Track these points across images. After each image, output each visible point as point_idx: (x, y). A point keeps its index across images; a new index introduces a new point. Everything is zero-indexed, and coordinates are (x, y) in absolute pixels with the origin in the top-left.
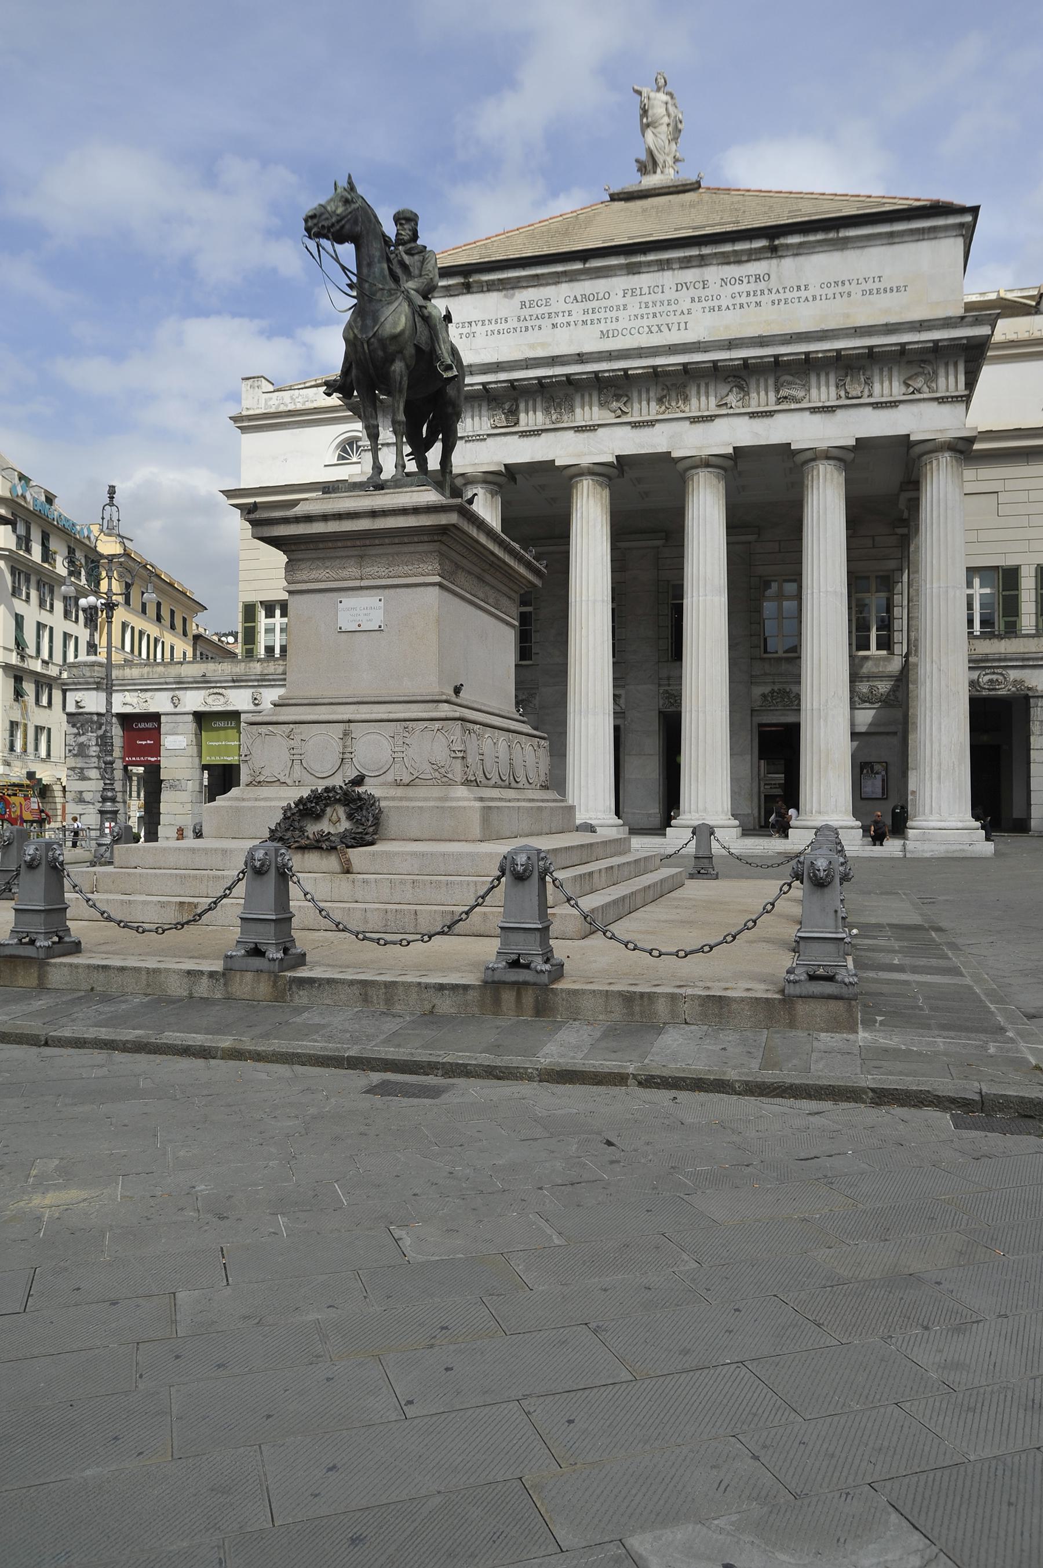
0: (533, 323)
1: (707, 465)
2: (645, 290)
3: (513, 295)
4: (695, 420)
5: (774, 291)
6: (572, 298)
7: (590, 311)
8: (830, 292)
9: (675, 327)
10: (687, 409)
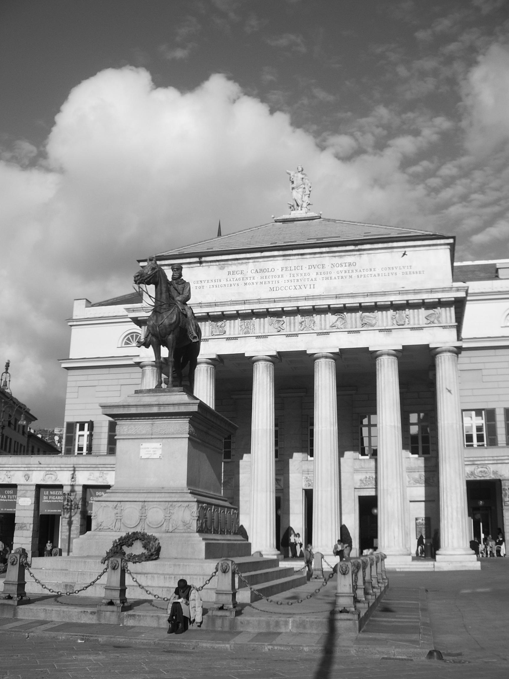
1: (326, 357)
2: (293, 268)
3: (224, 268)
4: (319, 334)
5: (358, 271)
6: (255, 271)
7: (264, 277)
8: (386, 272)
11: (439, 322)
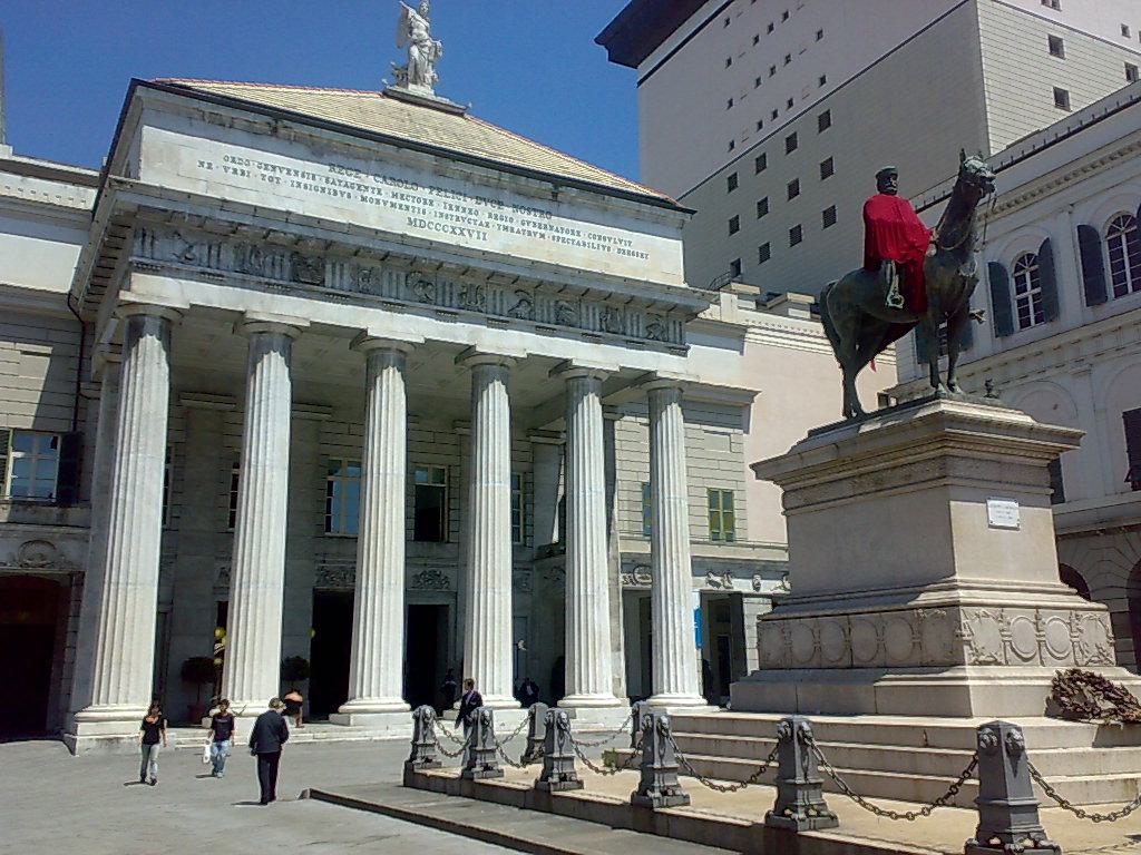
11: (667, 341)
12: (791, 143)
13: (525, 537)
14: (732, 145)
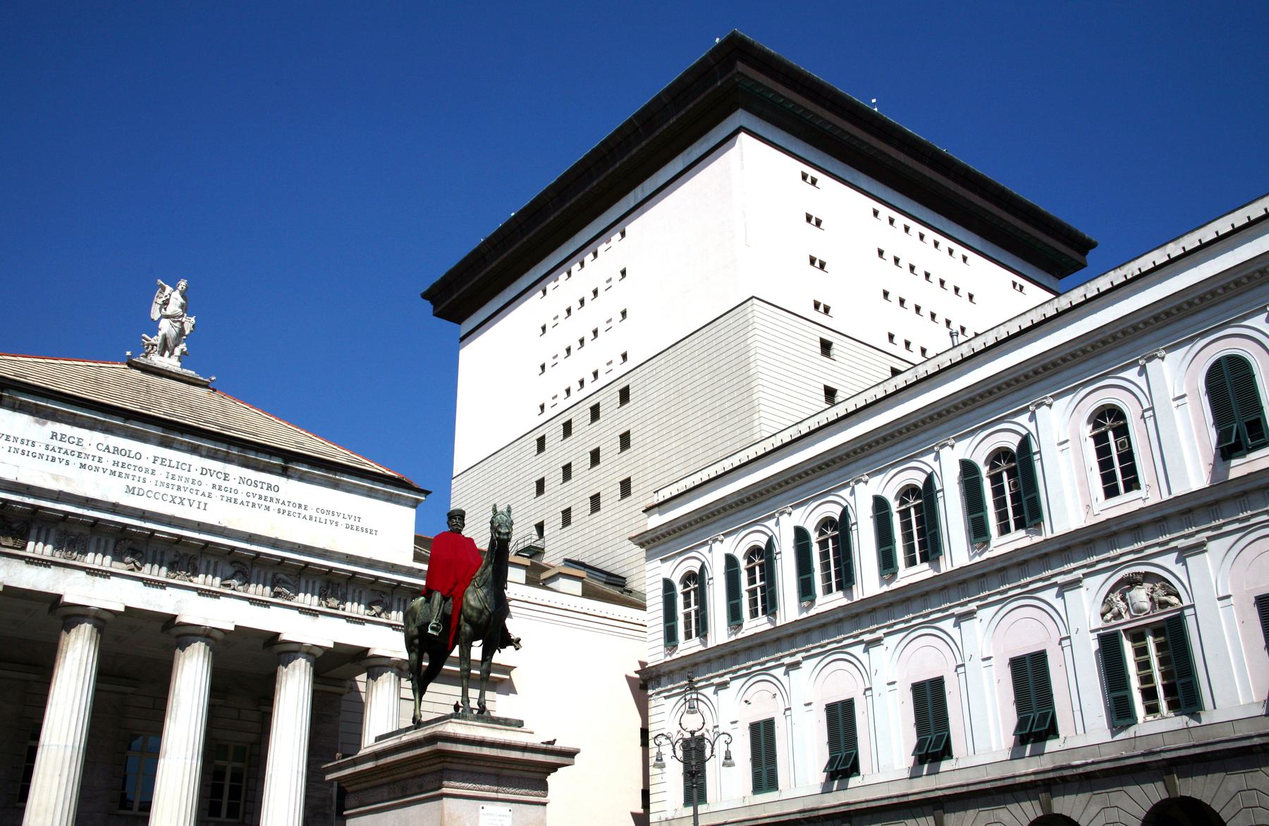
0: (62, 456)
3: (44, 424)
9: (196, 504)
10: (195, 579)
12: (595, 412)
13: (245, 813)
14: (542, 407)
